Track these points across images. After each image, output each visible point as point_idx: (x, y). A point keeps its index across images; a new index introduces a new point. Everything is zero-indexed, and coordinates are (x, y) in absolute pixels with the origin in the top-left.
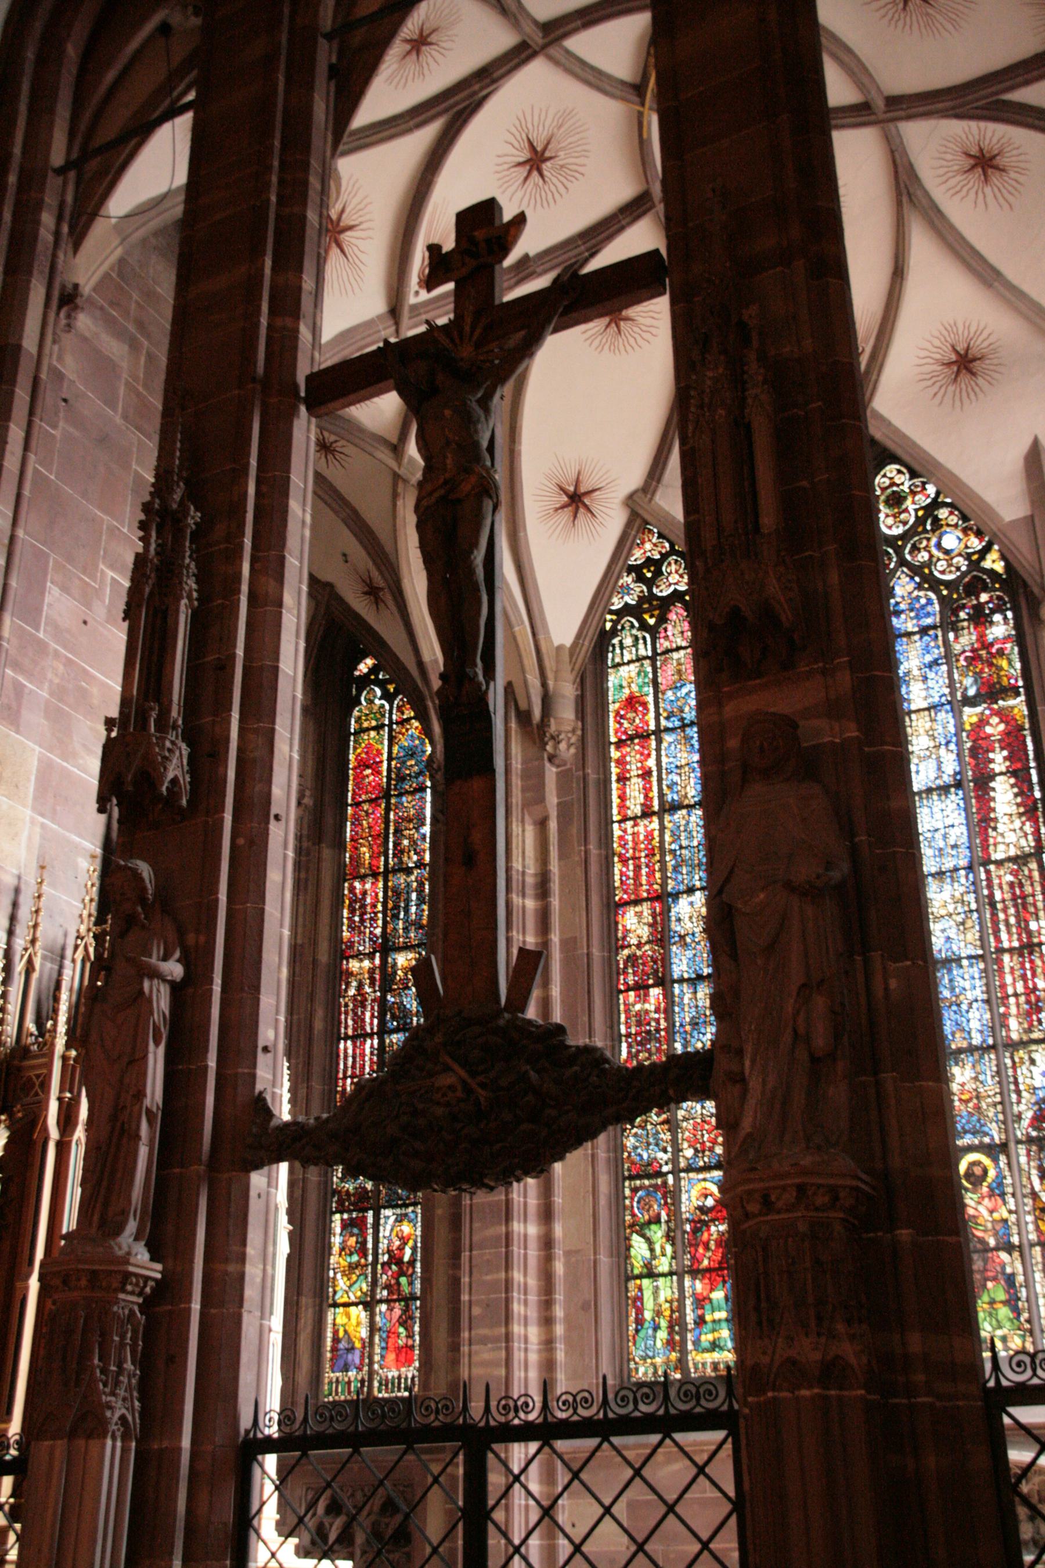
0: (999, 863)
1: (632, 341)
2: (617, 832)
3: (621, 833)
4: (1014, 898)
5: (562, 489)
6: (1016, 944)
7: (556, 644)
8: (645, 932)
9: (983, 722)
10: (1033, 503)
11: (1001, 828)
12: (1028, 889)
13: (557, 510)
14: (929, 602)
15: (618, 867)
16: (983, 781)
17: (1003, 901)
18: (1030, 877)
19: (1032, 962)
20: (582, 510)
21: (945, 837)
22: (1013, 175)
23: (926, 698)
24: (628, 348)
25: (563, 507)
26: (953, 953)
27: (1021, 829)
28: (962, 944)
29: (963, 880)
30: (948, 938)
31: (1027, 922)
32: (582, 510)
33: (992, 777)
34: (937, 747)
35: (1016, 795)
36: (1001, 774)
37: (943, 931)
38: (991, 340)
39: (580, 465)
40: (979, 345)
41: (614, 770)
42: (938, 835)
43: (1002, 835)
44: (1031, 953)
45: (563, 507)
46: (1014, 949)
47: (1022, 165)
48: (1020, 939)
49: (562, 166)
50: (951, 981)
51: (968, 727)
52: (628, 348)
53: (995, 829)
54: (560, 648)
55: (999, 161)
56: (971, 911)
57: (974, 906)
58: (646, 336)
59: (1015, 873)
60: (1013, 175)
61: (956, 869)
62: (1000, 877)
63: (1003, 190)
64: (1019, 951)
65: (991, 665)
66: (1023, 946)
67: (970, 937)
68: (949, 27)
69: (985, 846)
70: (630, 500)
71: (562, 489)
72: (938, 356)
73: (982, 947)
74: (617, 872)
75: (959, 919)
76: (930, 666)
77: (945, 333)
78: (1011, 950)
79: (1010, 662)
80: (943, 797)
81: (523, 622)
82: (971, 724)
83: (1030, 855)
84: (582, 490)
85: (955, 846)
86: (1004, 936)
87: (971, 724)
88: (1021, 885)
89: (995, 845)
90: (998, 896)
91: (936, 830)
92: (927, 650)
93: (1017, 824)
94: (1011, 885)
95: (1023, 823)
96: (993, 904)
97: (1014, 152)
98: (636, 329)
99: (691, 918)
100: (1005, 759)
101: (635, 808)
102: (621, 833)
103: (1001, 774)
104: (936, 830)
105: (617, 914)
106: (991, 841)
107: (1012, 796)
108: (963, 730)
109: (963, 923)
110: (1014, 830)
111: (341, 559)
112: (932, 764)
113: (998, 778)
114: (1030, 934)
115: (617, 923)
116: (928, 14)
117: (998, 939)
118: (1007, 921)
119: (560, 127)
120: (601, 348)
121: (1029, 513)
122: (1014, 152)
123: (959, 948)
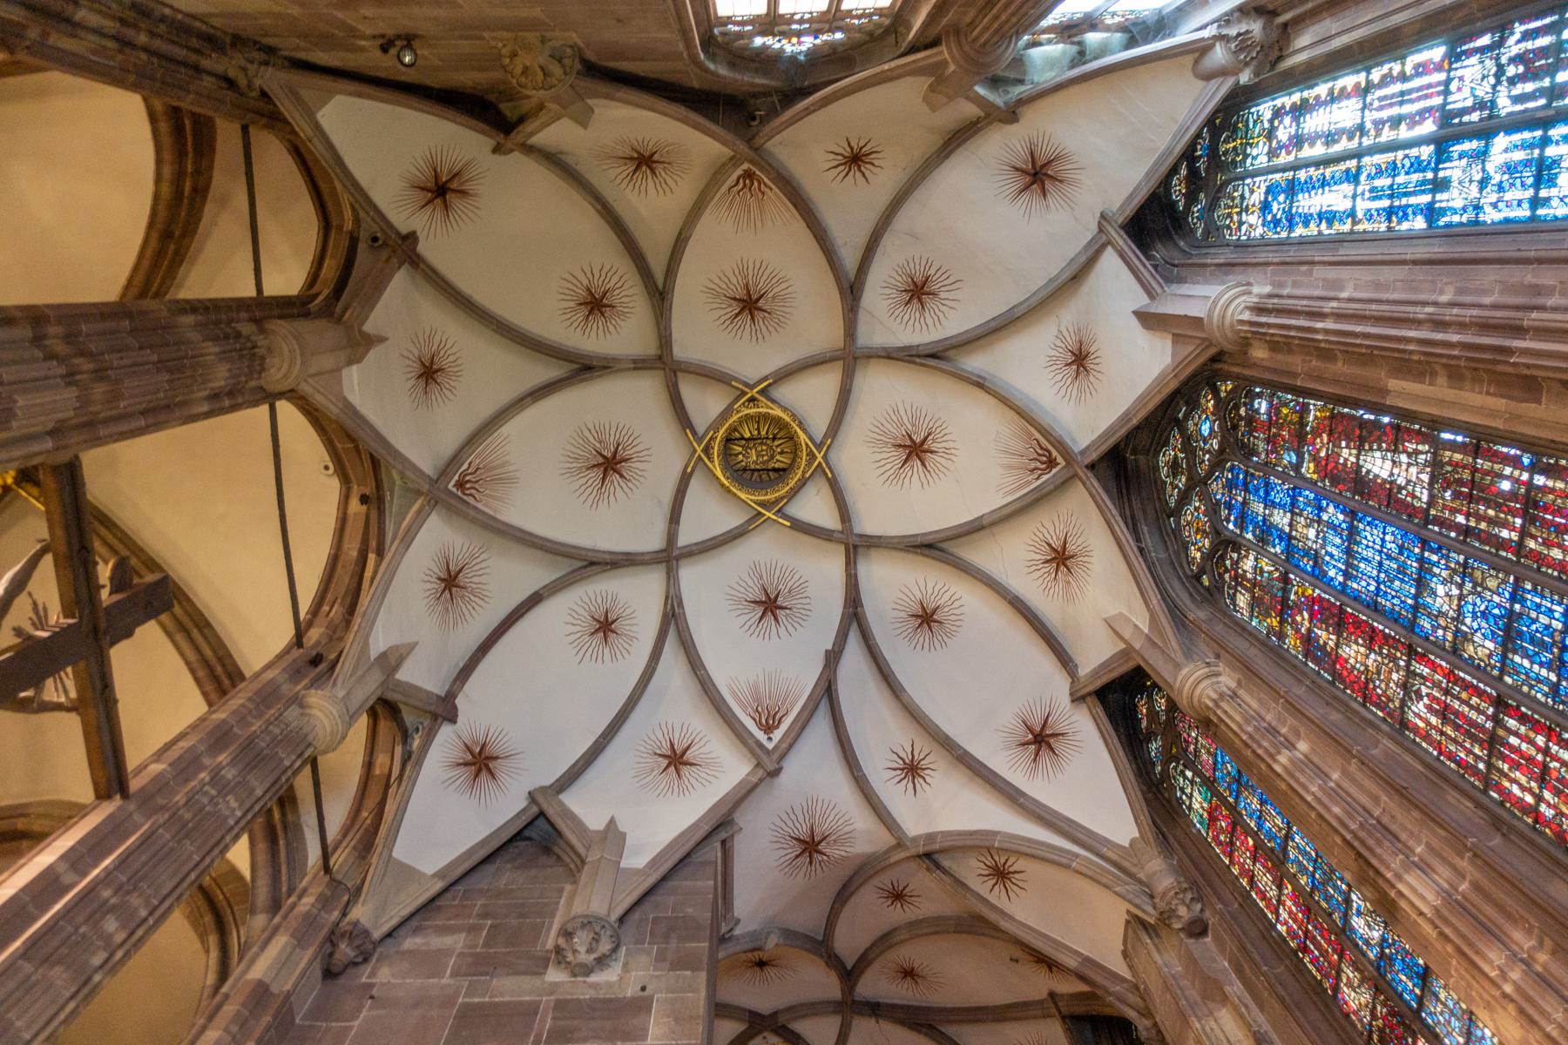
0: (1432, 502)
1: (953, 618)
2: (1282, 929)
3: (1285, 928)
4: (1470, 498)
5: (1023, 744)
6: (1518, 521)
7: (1127, 845)
8: (1365, 997)
9: (1315, 458)
10: (1166, 330)
11: (1401, 481)
12: (1466, 475)
13: (1035, 760)
14: (1231, 470)
15: (1307, 960)
16: (1361, 483)
17: (1468, 515)
18: (1456, 465)
19: (1546, 509)
20: (1052, 741)
21: (1389, 557)
22: (932, 272)
23: (1285, 512)
24: (958, 623)
25: (1037, 754)
26: (1502, 617)
27: (1409, 455)
28: (1496, 599)
29: (1435, 558)
30: (1483, 613)
31: (1501, 493)
32: (1052, 741)
33: (1359, 467)
34: (1319, 521)
35: (1379, 449)
36: (1358, 458)
37: (1475, 618)
38: (1071, 330)
39: (1019, 717)
40: (1072, 343)
41: (1244, 882)
42: (1386, 562)
43: (1409, 481)
44: (1536, 505)
45: (1037, 754)
46: (1523, 526)
47: (923, 264)
48: (1514, 514)
49: (790, 592)
50: (1532, 641)
51: (1315, 477)
52: (958, 623)
53: (1400, 488)
54: (1133, 842)
55: (919, 278)
56: (1465, 565)
57: (1461, 558)
58: (956, 604)
59: (1447, 485)
60: (932, 272)
61: (1421, 560)
62: (1445, 507)
63: (945, 283)
64: (1530, 519)
65: (1281, 428)
66: (1524, 514)
67: (1492, 583)
68: (784, 286)
69: (1412, 511)
70: (1077, 698)
71: (1023, 744)
72: (1070, 380)
73: (1508, 574)
74: (1310, 966)
75: (1469, 586)
76: (1267, 493)
77: (1055, 367)
78: (1524, 533)
79: (1286, 405)
80: (1358, 538)
81: (1077, 856)
82: (1314, 472)
83: (1435, 454)
84: (1038, 729)
85: (1401, 553)
86: (1505, 534)
87: (1314, 472)
88: (1460, 482)
89: (1414, 496)
90: (1461, 519)
91: (1380, 564)
92: (1257, 490)
93: (1404, 458)
94: (1457, 495)
95: (1405, 451)
96: (1467, 531)
97: (912, 265)
98: (946, 609)
99: (1369, 926)
100: (1348, 447)
101: (1272, 893)
102: (1285, 928)
103: (1358, 458)
104: (1380, 564)
105: (1341, 1008)
106: (1409, 499)
107: (1378, 454)
108: (1316, 483)
109: (1475, 584)
110: (1409, 465)
111: (1013, 964)
112: (1331, 535)
113: (1361, 463)
114: (1513, 496)
115: (1347, 1015)
116: (773, 297)
117: (1503, 544)
118: (1490, 521)
119: (761, 578)
120: (944, 644)
121: (1170, 336)
122: (912, 265)
123: (1499, 606)
